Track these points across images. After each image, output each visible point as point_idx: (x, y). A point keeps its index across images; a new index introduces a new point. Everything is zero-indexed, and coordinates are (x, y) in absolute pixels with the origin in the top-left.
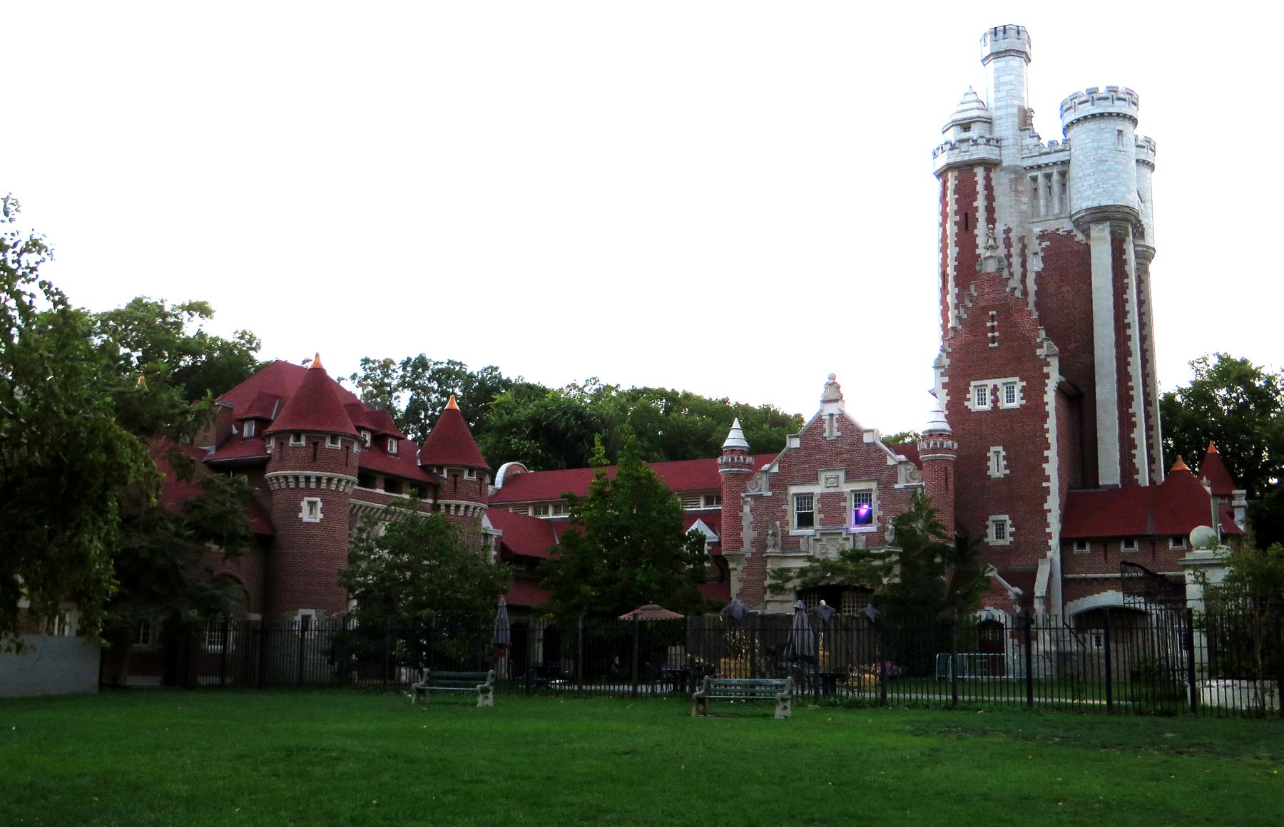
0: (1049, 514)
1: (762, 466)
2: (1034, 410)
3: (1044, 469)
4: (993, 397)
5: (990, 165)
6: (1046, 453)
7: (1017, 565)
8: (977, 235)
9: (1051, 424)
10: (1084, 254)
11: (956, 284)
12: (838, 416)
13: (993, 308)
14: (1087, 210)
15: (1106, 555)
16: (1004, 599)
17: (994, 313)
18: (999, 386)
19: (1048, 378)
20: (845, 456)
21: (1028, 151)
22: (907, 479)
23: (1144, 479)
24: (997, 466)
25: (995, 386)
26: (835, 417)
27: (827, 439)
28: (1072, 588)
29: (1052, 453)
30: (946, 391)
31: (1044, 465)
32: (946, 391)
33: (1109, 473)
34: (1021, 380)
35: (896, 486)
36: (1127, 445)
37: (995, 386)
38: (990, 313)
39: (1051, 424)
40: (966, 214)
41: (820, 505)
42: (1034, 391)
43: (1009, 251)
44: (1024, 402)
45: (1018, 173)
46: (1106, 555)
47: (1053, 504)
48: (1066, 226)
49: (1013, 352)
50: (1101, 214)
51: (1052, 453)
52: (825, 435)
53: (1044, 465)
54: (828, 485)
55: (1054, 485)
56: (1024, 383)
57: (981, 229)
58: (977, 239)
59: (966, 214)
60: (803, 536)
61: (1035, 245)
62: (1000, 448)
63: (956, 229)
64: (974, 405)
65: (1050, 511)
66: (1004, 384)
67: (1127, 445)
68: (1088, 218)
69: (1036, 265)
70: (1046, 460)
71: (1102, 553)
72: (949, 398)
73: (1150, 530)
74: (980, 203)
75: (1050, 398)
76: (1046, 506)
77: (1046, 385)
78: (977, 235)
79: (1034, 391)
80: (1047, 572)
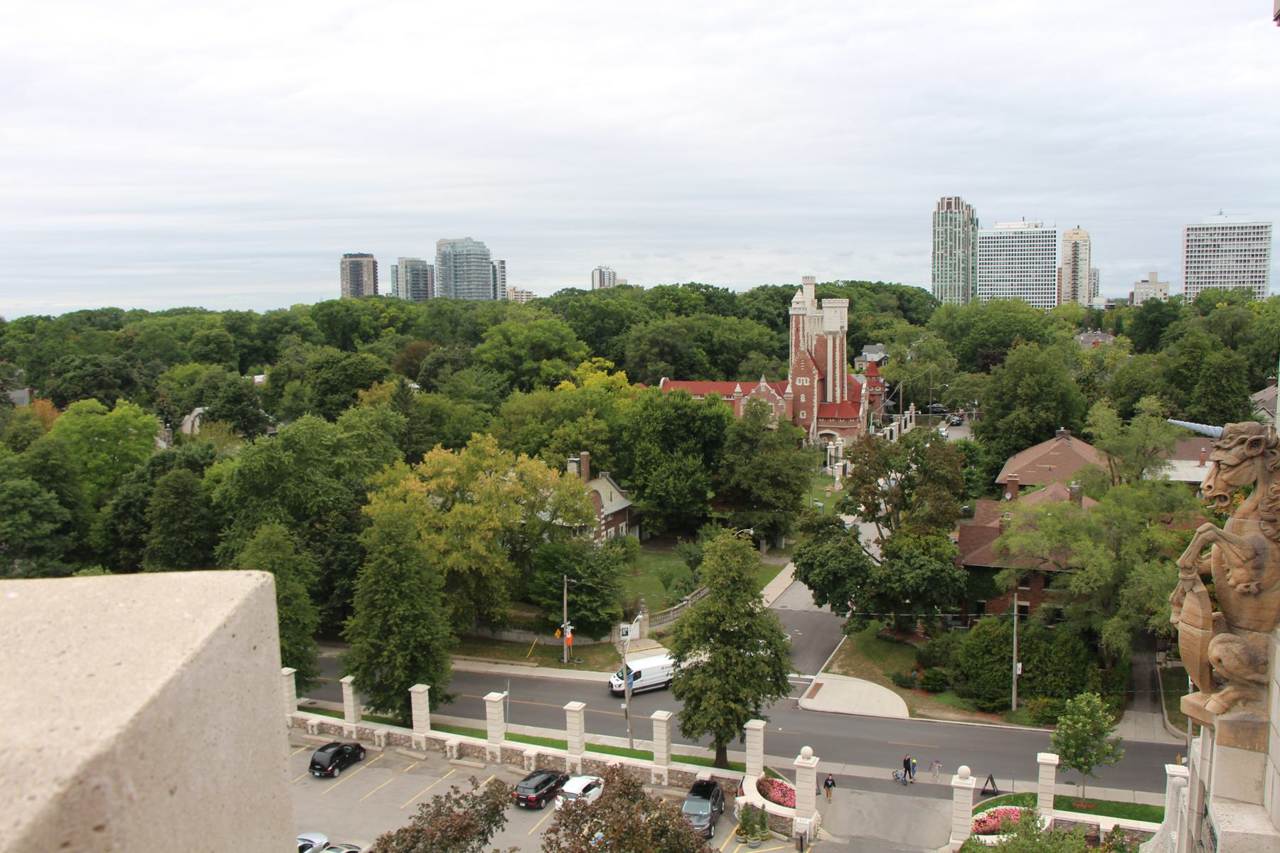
2: (812, 386)
5: (803, 315)
7: (807, 423)
9: (816, 390)
10: (826, 342)
23: (838, 401)
24: (803, 399)
28: (819, 429)
29: (815, 397)
33: (830, 399)
36: (834, 391)
39: (816, 390)
42: (812, 382)
45: (811, 318)
47: (815, 409)
48: (822, 333)
50: (830, 333)
51: (815, 397)
55: (816, 405)
57: (801, 333)
61: (815, 338)
64: (798, 383)
67: (834, 391)
69: (814, 342)
73: (836, 416)
74: (801, 326)
75: (816, 384)
79: (812, 382)
80: (814, 425)
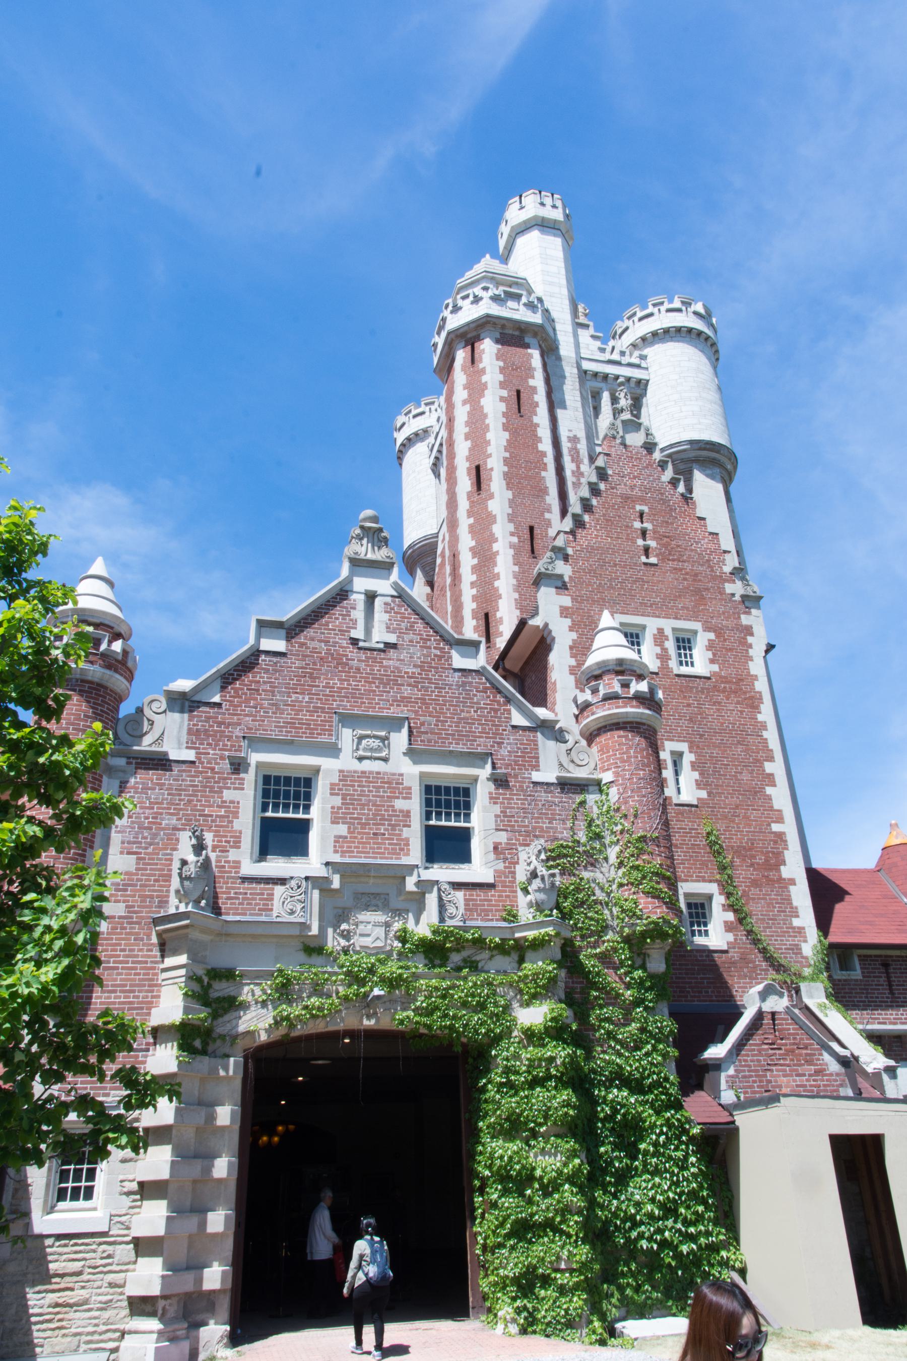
0: (792, 888)
1: (175, 680)
3: (769, 798)
4: (658, 650)
6: (769, 767)
8: (537, 425)
11: (508, 484)
12: (389, 599)
13: (643, 501)
14: (691, 442)
15: (890, 985)
16: (819, 1072)
17: (645, 509)
18: (668, 632)
19: (752, 634)
20: (407, 691)
21: (589, 352)
22: (561, 765)
25: (661, 631)
26: (378, 602)
27: (361, 644)
30: (568, 622)
31: (769, 790)
32: (568, 622)
34: (707, 629)
35: (536, 776)
37: (661, 631)
38: (638, 508)
40: (518, 392)
41: (337, 801)
43: (578, 467)
44: (715, 668)
46: (890, 985)
49: (685, 579)
52: (354, 634)
53: (769, 790)
54: (361, 753)
56: (712, 636)
58: (538, 429)
59: (518, 392)
60: (282, 881)
62: (683, 747)
63: (503, 407)
65: (792, 882)
66: (674, 630)
68: (692, 454)
70: (770, 779)
71: (883, 980)
72: (574, 635)
76: (785, 872)
77: (750, 646)
78: (537, 425)
